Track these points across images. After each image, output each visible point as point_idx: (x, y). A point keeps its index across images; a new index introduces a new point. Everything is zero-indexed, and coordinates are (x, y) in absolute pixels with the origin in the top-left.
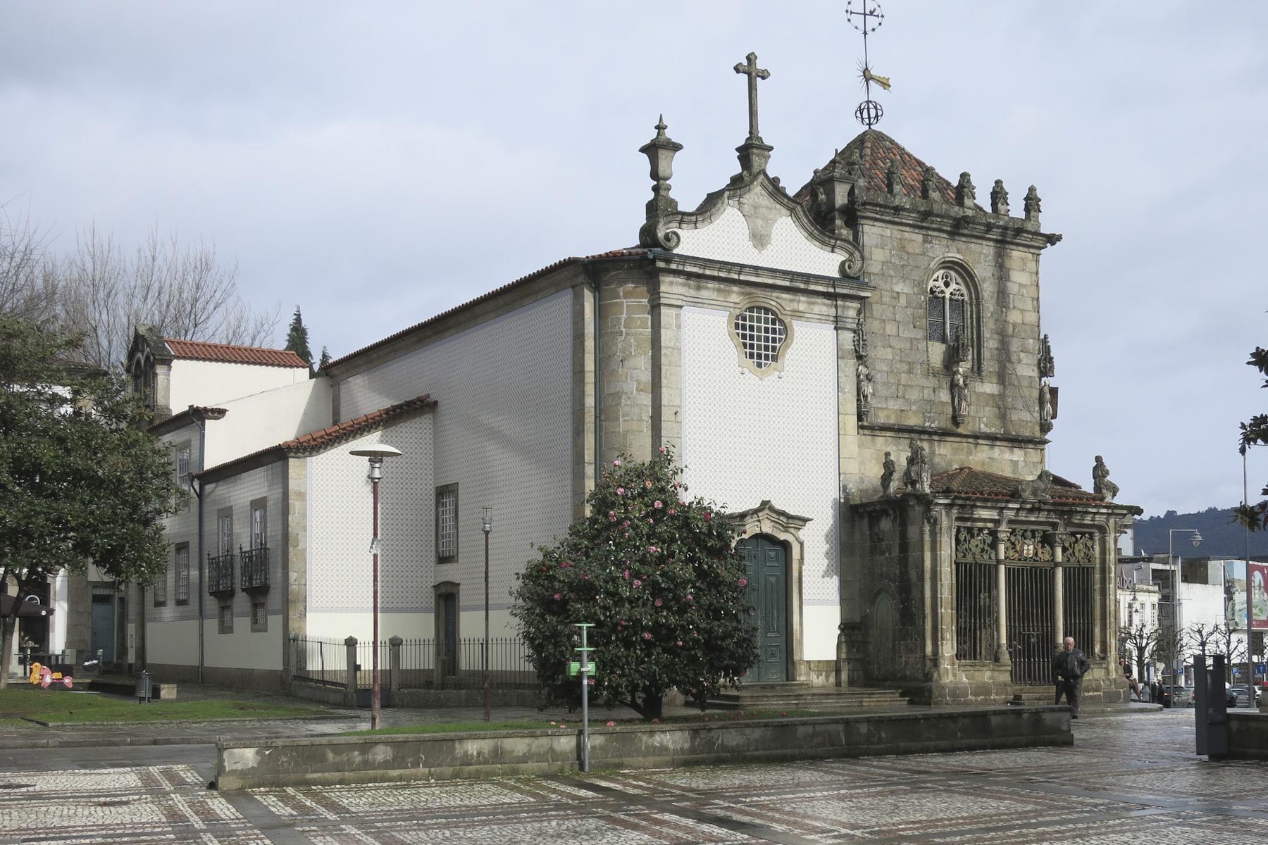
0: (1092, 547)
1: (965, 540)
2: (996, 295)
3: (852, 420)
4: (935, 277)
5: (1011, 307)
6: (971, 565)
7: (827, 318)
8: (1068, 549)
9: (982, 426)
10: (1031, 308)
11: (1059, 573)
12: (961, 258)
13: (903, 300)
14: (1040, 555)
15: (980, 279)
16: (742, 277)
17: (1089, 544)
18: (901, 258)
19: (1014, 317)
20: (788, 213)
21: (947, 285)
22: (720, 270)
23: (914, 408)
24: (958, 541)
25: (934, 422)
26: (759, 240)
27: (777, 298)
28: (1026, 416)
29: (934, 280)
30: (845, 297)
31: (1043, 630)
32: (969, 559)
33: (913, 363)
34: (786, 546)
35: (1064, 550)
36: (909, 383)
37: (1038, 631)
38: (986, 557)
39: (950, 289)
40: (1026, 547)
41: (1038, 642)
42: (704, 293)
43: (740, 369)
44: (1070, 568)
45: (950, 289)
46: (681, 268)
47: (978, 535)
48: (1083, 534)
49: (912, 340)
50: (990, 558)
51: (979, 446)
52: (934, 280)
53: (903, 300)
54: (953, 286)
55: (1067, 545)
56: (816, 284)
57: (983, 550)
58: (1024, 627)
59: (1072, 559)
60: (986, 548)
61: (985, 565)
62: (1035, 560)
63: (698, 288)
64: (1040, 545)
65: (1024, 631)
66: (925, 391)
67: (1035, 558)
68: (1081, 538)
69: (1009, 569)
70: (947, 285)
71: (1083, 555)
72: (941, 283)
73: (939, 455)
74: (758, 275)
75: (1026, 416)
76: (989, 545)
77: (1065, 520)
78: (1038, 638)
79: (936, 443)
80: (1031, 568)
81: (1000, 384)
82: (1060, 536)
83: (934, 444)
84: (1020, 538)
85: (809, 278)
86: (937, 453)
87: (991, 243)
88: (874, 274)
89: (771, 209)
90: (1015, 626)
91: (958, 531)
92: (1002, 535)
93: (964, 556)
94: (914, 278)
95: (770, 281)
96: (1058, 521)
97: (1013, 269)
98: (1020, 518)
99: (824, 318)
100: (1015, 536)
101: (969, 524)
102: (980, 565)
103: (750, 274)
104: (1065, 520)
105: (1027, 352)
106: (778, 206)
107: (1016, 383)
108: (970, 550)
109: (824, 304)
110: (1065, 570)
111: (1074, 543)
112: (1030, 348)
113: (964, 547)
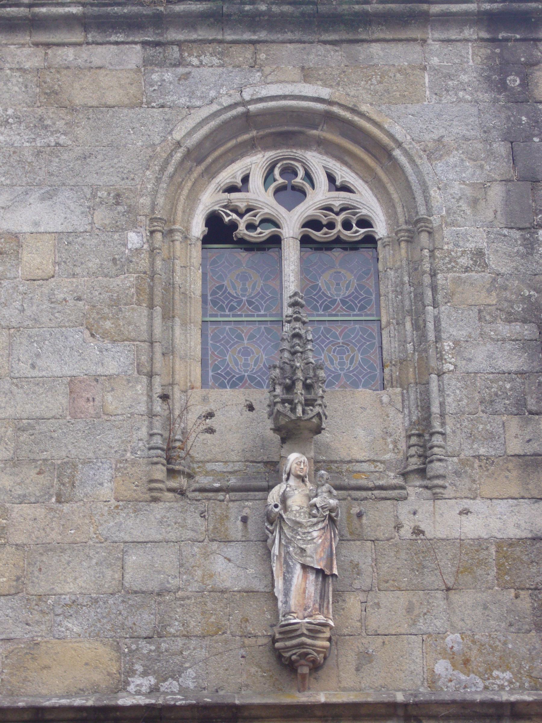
12: (325, 93)
15: (415, 148)
25: (175, 675)
29: (232, 189)
36: (54, 536)
52: (232, 189)
66: (132, 559)
87: (469, 33)
94: (93, 179)
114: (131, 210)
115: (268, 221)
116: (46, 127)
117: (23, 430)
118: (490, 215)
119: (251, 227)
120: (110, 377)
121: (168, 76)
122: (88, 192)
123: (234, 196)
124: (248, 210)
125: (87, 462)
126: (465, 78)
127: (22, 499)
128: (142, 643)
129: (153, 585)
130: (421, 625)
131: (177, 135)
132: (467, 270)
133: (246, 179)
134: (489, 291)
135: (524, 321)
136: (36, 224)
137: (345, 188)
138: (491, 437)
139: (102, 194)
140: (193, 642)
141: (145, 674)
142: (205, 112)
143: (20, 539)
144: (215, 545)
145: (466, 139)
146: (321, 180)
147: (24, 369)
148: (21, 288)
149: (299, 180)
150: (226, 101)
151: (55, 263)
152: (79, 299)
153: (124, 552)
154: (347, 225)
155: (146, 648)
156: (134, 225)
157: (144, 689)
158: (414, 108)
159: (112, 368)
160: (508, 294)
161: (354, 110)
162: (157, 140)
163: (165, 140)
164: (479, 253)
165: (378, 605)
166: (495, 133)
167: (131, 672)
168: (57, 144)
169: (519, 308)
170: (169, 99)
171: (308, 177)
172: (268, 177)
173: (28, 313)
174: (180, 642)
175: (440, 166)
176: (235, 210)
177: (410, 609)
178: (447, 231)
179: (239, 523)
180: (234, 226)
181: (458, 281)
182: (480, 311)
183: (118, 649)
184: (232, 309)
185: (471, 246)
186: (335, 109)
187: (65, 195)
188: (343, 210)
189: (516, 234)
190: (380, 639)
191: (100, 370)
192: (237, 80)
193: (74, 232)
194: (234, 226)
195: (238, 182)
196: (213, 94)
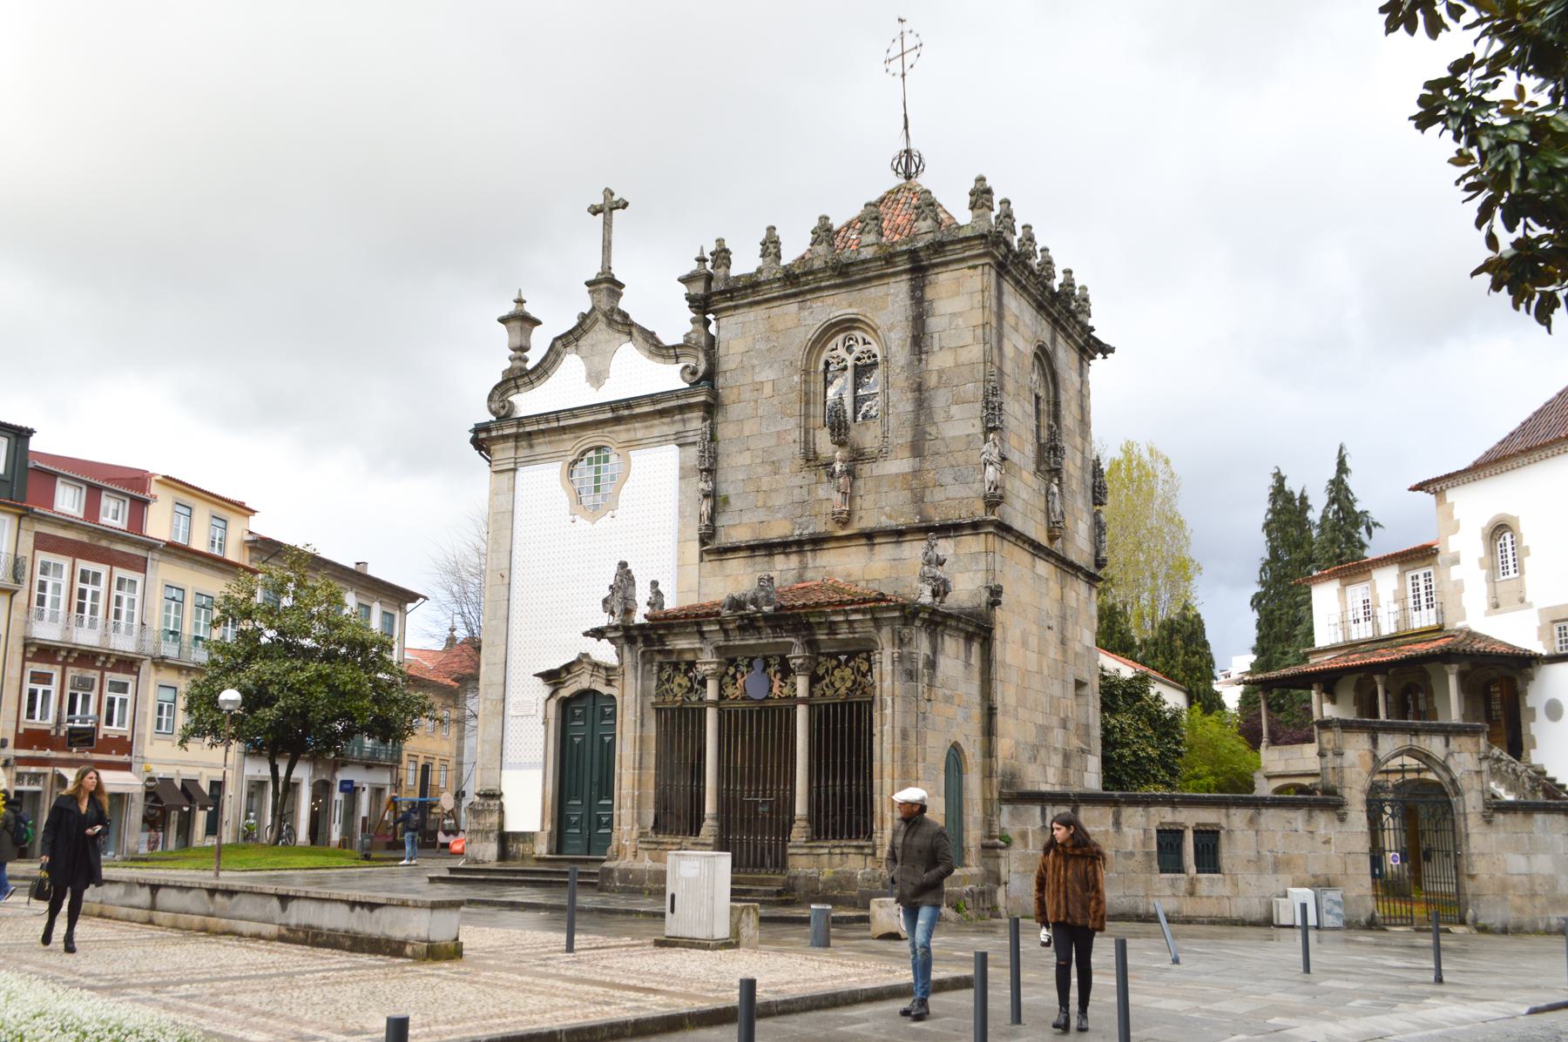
0: (870, 670)
1: (668, 680)
3: (695, 547)
4: (831, 345)
5: (936, 348)
6: (672, 710)
7: (668, 438)
8: (823, 678)
9: (883, 519)
10: (970, 341)
11: (802, 713)
13: (768, 390)
14: (776, 690)
16: (562, 424)
17: (864, 667)
18: (768, 339)
19: (939, 361)
20: (628, 338)
22: (538, 423)
24: (659, 679)
25: (807, 528)
26: (596, 378)
27: (610, 432)
28: (956, 491)
30: (682, 409)
31: (778, 794)
33: (779, 461)
34: (612, 697)
35: (814, 680)
37: (771, 796)
38: (694, 698)
39: (857, 353)
41: (771, 812)
42: (538, 450)
43: (571, 517)
44: (827, 706)
46: (500, 433)
47: (686, 673)
48: (852, 656)
51: (877, 547)
52: (833, 350)
53: (768, 390)
54: (858, 349)
55: (821, 671)
56: (639, 405)
57: (691, 689)
59: (829, 692)
61: (693, 709)
63: (531, 446)
64: (779, 676)
68: (847, 661)
69: (729, 712)
70: (849, 349)
71: (849, 684)
72: (841, 352)
74: (575, 416)
75: (956, 491)
76: (700, 683)
77: (804, 637)
78: (771, 808)
79: (809, 554)
81: (915, 457)
82: (794, 661)
84: (745, 669)
85: (628, 403)
86: (810, 566)
87: (905, 277)
89: (609, 341)
90: (735, 790)
91: (661, 668)
92: (704, 668)
94: (784, 358)
95: (590, 419)
96: (793, 640)
97: (941, 298)
98: (731, 643)
99: (664, 439)
100: (737, 667)
101: (674, 659)
103: (566, 418)
106: (617, 335)
107: (943, 449)
108: (672, 690)
109: (664, 424)
110: (811, 707)
112: (970, 396)
114: (796, 367)
115: (843, 360)
121: (806, 313)
126: (901, 296)
131: (809, 337)
142: (818, 326)
147: (764, 431)
154: (869, 358)
155: (799, 520)
158: (885, 312)
161: (865, 316)
167: (794, 529)
178: (893, 360)
186: (859, 317)
187: (776, 365)
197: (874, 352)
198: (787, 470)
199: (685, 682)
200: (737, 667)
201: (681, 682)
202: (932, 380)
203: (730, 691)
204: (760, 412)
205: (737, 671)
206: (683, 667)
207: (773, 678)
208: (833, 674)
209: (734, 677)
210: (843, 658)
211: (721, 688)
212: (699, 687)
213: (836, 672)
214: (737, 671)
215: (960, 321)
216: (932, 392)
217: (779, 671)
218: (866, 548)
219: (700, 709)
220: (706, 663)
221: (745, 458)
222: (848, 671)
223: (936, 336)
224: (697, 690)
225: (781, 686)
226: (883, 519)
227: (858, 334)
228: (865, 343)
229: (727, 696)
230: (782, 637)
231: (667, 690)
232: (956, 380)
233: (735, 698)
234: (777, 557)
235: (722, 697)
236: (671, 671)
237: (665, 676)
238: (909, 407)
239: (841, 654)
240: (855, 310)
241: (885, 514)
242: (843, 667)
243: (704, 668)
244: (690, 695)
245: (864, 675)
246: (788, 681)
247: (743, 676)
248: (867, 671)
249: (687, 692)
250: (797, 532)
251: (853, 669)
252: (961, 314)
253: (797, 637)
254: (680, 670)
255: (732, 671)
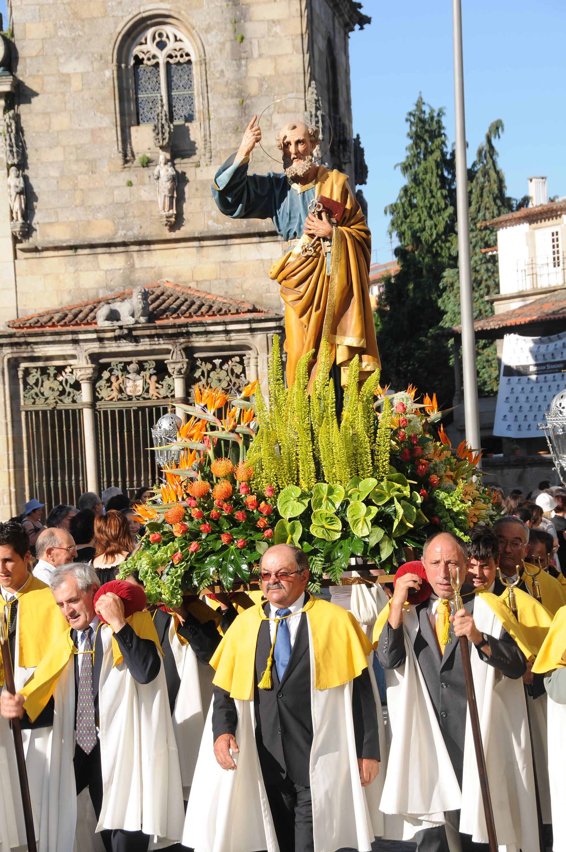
0: (244, 372)
1: (36, 384)
2: (228, 46)
5: (256, 55)
6: (45, 412)
8: (199, 380)
9: (210, 222)
13: (76, 84)
14: (152, 391)
17: (238, 369)
18: (72, 28)
21: (161, 45)
23: (100, 215)
25: (131, 229)
32: (40, 405)
38: (67, 400)
40: (129, 384)
45: (167, 51)
47: (55, 376)
48: (226, 359)
49: (93, 132)
50: (74, 401)
53: (76, 84)
54: (171, 45)
57: (63, 393)
58: (131, 481)
60: (68, 389)
61: (67, 411)
62: (145, 399)
64: (154, 378)
65: (132, 485)
66: (116, 192)
67: (145, 396)
68: (222, 365)
70: (161, 45)
71: (224, 384)
72: (151, 47)
73: (141, 268)
76: (71, 386)
79: (135, 255)
80: (139, 408)
82: (173, 366)
83: (132, 257)
84: (119, 373)
86: (137, 265)
88: (31, 57)
92: (79, 373)
93: (34, 403)
96: (170, 347)
98: (107, 350)
100: (111, 371)
101: (40, 364)
102: (60, 412)
104: (181, 344)
105: (286, 111)
108: (42, 394)
111: (209, 372)
113: (33, 392)
114: (106, 62)
115: (154, 57)
116: (74, 28)
117: (79, 148)
118: (226, 55)
119: (149, 59)
120: (104, 128)
122: (90, 55)
123: (143, 47)
124: (148, 52)
125: (100, 159)
127: (81, 173)
128: (121, 220)
129: (123, 201)
130: (204, 209)
131: (119, 29)
132: (218, 78)
133: (146, 40)
134: (226, 86)
135: (237, 97)
136: (75, 69)
137: (181, 40)
138: (226, 142)
139: (96, 55)
140: (136, 219)
141: (123, 230)
143: (81, 187)
144: (141, 186)
145: (218, 23)
146: (172, 38)
148: (73, 95)
149: (164, 39)
150: (135, 13)
151: (83, 85)
152: (92, 98)
153: (113, 190)
154: (182, 56)
155: (122, 221)
156: (107, 67)
157: (123, 235)
159: (104, 125)
160: (231, 87)
162: (112, 31)
163: (115, 30)
164: (222, 71)
165: (191, 203)
166: (228, 20)
167: (118, 230)
168: (79, 35)
169: (235, 92)
170: (116, 13)
171: (168, 37)
172: (154, 39)
173: (76, 105)
174: (132, 219)
175: (209, 36)
176: (143, 53)
177: (201, 204)
179: (148, 178)
180: (143, 59)
181: (216, 83)
182: (223, 94)
183: (114, 222)
184: (146, 91)
185: (220, 69)
188: (180, 49)
189: (234, 62)
190: (191, 215)
191: (101, 125)
192: (138, 3)
193: (88, 73)
194: (143, 59)
195: (143, 41)
196: (130, 10)
197: (187, 50)
198: (106, 170)
199: (56, 385)
200: (111, 371)
201: (52, 385)
202: (253, 88)
203: (104, 393)
204: (70, 106)
205: (111, 375)
206: (52, 372)
207: (148, 381)
208: (208, 376)
209: (109, 380)
210: (217, 362)
211: (94, 391)
212: (71, 390)
213: (212, 374)
214: (111, 375)
215: (277, 29)
216: (254, 100)
217: (154, 374)
218: (194, 250)
219: (74, 411)
220: (81, 369)
221: (57, 155)
222: (223, 374)
223: (255, 42)
224: (69, 393)
225: (157, 388)
226: (210, 222)
227: (167, 30)
228: (176, 40)
229: (102, 398)
230: (159, 344)
231: (37, 395)
232: (277, 89)
233: (111, 400)
234: (100, 256)
235: (95, 399)
236: (38, 375)
237: (31, 380)
238: (233, 113)
239: (215, 358)
240: (168, 6)
241: (212, 218)
242: (218, 370)
243: (79, 373)
244: (62, 397)
245: (238, 377)
246: (164, 383)
247: (118, 378)
248: (241, 373)
249: (60, 395)
250: (124, 232)
251: (227, 371)
252: (279, 21)
253: (172, 345)
254: (49, 375)
255: (106, 375)
